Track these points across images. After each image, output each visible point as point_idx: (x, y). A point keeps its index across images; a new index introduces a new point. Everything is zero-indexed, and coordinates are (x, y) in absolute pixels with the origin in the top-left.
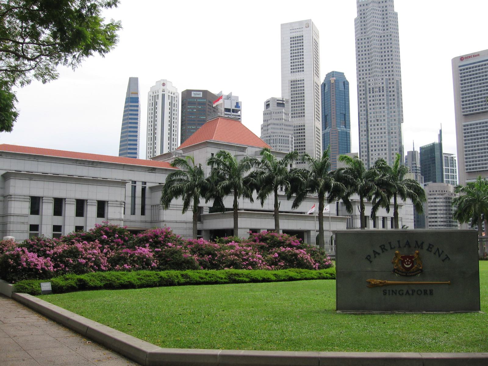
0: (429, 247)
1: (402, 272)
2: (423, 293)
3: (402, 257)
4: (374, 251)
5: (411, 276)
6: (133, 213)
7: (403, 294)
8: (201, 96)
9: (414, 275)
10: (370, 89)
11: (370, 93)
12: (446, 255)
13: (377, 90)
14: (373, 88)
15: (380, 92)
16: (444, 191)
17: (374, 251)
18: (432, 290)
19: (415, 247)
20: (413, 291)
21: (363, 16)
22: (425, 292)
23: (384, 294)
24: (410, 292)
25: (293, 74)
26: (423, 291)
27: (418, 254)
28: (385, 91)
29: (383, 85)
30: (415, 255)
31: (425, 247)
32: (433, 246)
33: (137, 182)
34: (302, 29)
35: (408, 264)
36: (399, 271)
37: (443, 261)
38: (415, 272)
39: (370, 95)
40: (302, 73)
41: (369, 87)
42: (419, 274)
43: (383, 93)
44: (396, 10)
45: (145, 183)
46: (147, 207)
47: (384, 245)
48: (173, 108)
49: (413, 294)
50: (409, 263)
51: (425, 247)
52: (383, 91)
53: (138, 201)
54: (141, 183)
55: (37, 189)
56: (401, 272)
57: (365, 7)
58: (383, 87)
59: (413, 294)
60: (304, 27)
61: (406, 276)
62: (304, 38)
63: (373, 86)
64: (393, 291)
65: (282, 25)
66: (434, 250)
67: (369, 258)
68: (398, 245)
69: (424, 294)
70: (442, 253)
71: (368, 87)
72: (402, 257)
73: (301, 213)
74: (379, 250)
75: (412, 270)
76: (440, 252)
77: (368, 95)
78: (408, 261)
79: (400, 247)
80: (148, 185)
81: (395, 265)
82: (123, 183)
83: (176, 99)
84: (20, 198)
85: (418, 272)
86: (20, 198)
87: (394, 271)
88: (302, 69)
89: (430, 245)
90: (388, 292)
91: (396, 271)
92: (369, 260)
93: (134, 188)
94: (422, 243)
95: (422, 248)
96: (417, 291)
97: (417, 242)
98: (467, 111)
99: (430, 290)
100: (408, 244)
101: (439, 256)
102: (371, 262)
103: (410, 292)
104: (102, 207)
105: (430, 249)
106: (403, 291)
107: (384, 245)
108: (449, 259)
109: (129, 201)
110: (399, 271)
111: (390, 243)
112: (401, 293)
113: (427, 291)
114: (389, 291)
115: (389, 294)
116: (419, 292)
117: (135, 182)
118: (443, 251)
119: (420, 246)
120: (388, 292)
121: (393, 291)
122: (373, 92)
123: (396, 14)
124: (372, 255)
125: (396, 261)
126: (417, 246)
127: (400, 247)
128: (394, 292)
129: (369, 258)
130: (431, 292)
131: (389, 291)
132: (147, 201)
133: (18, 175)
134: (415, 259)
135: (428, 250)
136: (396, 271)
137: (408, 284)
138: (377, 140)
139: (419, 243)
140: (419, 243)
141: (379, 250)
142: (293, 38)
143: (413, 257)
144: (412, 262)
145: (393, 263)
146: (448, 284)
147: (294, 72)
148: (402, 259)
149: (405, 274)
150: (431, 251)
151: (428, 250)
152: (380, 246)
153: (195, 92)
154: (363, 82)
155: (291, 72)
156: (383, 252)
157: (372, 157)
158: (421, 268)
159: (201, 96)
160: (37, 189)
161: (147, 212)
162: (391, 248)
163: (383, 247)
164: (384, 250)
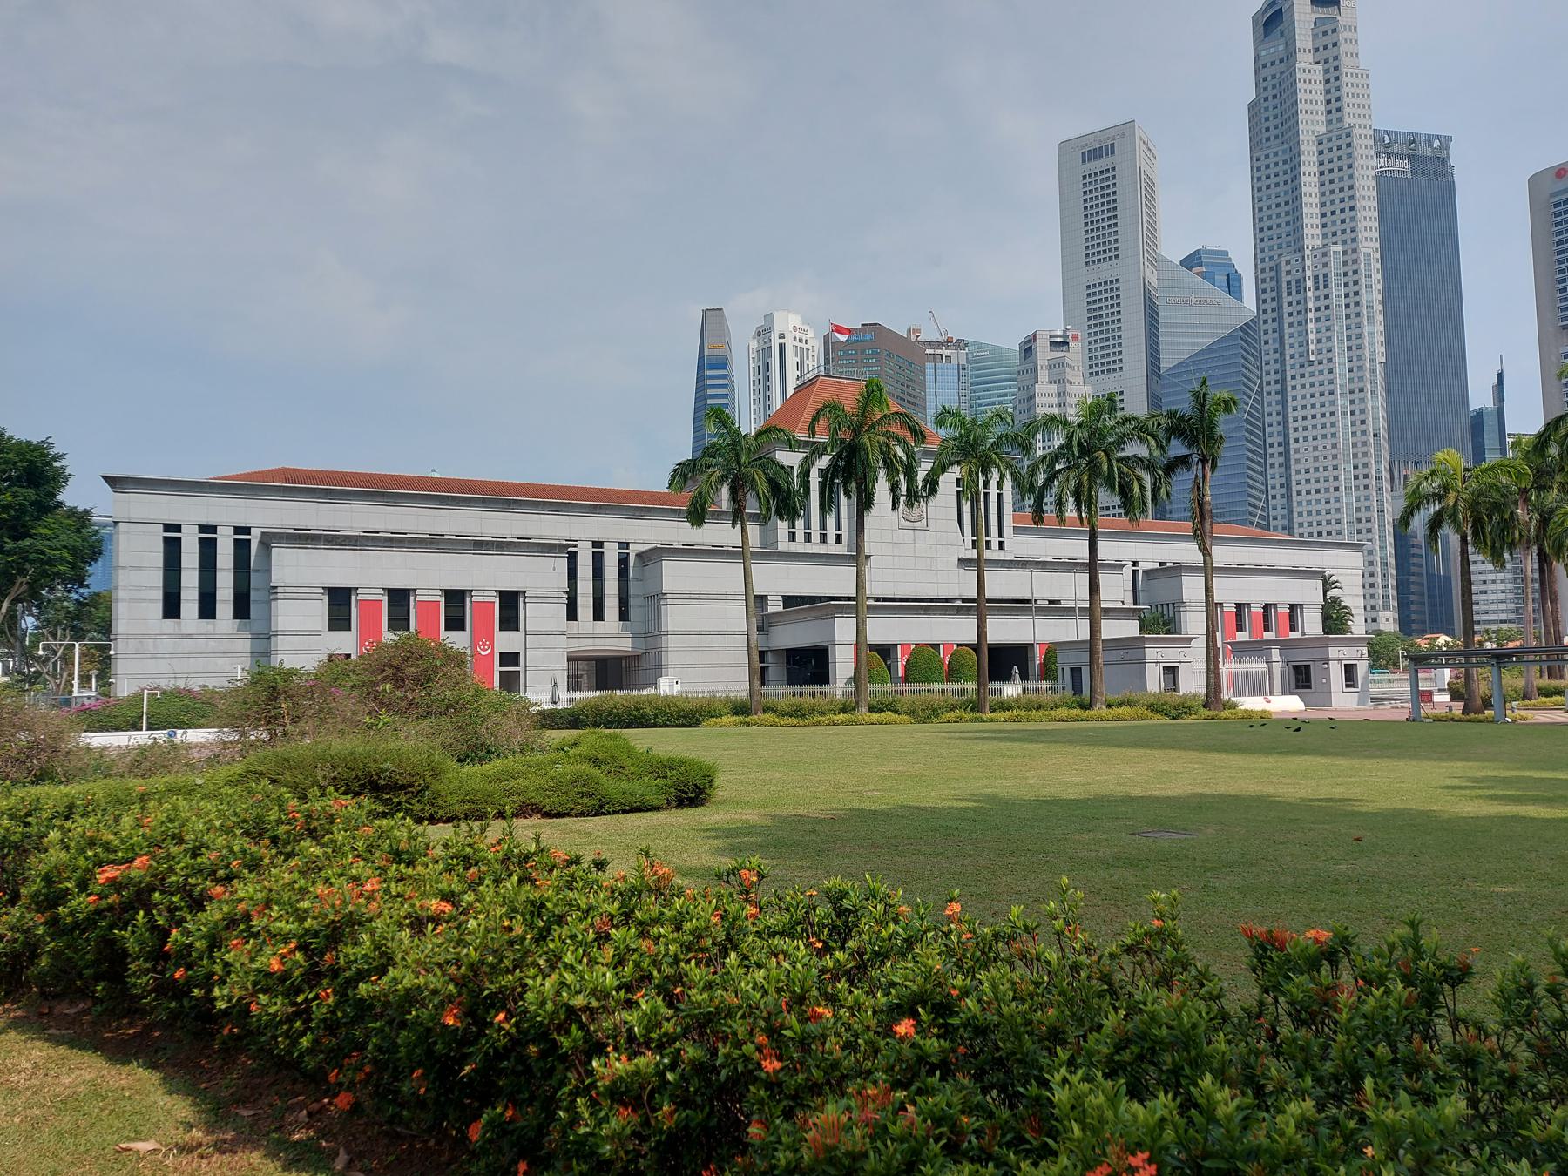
6: (598, 615)
10: (1289, 283)
11: (1289, 294)
13: (1309, 284)
14: (1298, 281)
15: (1317, 288)
29: (1325, 270)
39: (1290, 299)
41: (1289, 278)
43: (1326, 291)
46: (632, 602)
52: (1326, 286)
55: (341, 568)
58: (1326, 275)
63: (1299, 276)
71: (1285, 279)
73: (947, 600)
77: (1286, 299)
84: (301, 592)
86: (301, 592)
93: (598, 559)
109: (585, 588)
117: (598, 544)
122: (1298, 292)
132: (633, 589)
133: (304, 539)
154: (1271, 269)
160: (341, 568)
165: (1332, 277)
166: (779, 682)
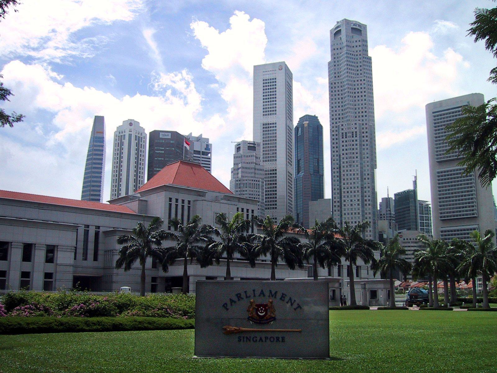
0: (282, 296)
4: (230, 299)
5: (265, 323)
7: (256, 340)
8: (170, 137)
10: (343, 133)
12: (298, 304)
14: (346, 133)
16: (407, 239)
17: (230, 299)
18: (284, 337)
19: (269, 296)
21: (336, 60)
22: (278, 339)
24: (264, 340)
25: (265, 117)
26: (275, 339)
27: (271, 303)
28: (358, 136)
29: (356, 130)
31: (279, 296)
32: (286, 295)
33: (90, 227)
34: (275, 72)
35: (261, 313)
37: (295, 309)
39: (343, 140)
40: (274, 116)
41: (342, 131)
43: (356, 138)
44: (369, 55)
45: (98, 227)
46: (100, 252)
47: (240, 294)
48: (140, 149)
49: (265, 341)
51: (279, 296)
52: (356, 136)
53: (91, 246)
54: (94, 227)
57: (339, 51)
58: (356, 132)
59: (265, 341)
60: (277, 69)
62: (277, 80)
65: (255, 67)
66: (287, 299)
67: (225, 306)
69: (277, 341)
71: (341, 131)
72: (257, 305)
74: (235, 299)
75: (265, 318)
76: (293, 302)
78: (262, 310)
79: (254, 296)
80: (102, 230)
82: (75, 228)
83: (143, 140)
87: (250, 319)
88: (274, 112)
89: (283, 294)
90: (242, 338)
93: (86, 233)
94: (276, 292)
95: (275, 297)
97: (271, 292)
98: (441, 158)
99: (282, 338)
100: (262, 293)
102: (227, 309)
103: (264, 340)
104: (51, 250)
105: (283, 299)
106: (256, 337)
107: (240, 294)
108: (301, 308)
109: (81, 245)
111: (246, 292)
115: (244, 341)
116: (272, 339)
117: (88, 226)
119: (273, 295)
120: (242, 338)
121: (247, 338)
122: (346, 137)
123: (370, 59)
124: (229, 303)
125: (251, 309)
127: (254, 296)
130: (283, 339)
132: (101, 246)
135: (281, 299)
137: (261, 331)
138: (349, 186)
139: (273, 292)
140: (273, 292)
141: (235, 299)
142: (266, 80)
143: (266, 305)
144: (266, 311)
145: (248, 311)
147: (266, 114)
149: (259, 322)
150: (283, 300)
152: (237, 295)
153: (163, 133)
155: (264, 115)
156: (239, 300)
157: (345, 203)
158: (274, 316)
159: (170, 137)
161: (100, 257)
162: (247, 297)
163: (239, 295)
165: (358, 133)
166: (162, 291)
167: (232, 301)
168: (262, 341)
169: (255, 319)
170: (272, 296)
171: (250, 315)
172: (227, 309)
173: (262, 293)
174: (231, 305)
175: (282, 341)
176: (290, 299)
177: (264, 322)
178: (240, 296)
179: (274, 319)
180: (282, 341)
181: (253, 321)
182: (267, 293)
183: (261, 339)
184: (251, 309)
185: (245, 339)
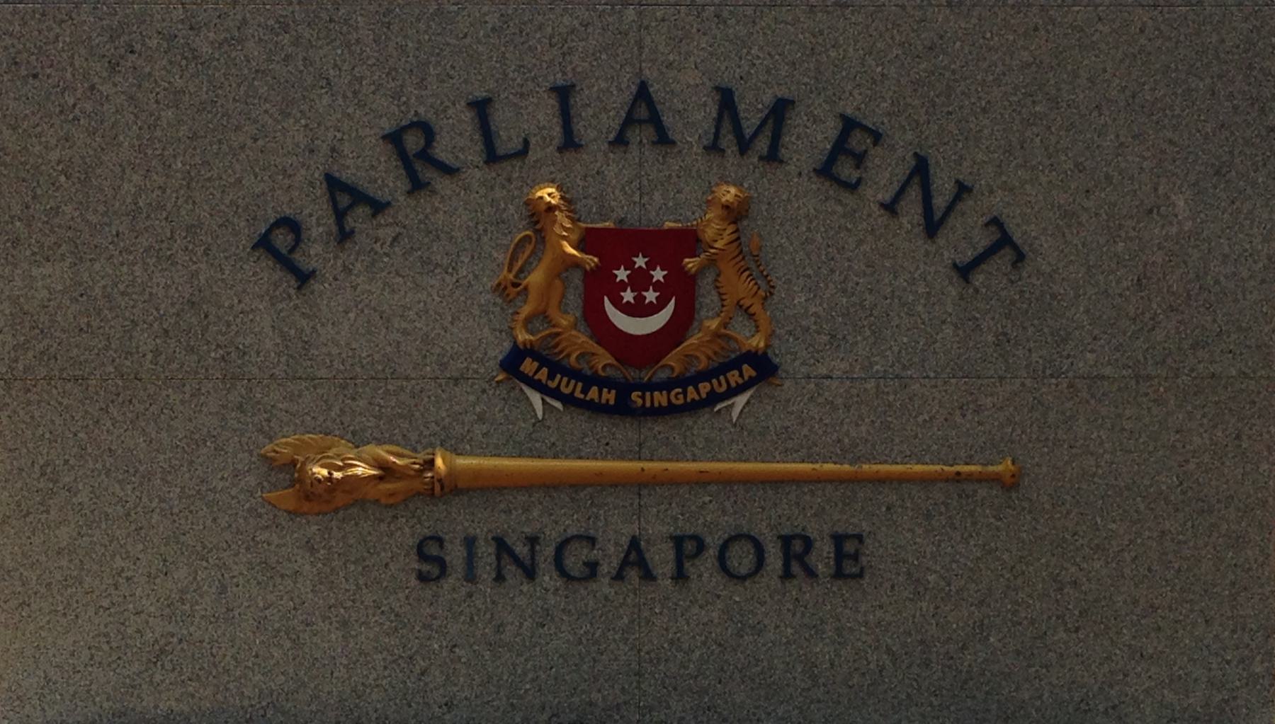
0: (840, 147)
1: (590, 380)
2: (774, 560)
3: (588, 241)
4: (334, 184)
5: (671, 410)
9: (692, 407)
12: (996, 222)
17: (334, 184)
20: (686, 548)
22: (796, 550)
23: (423, 578)
24: (661, 557)
27: (735, 214)
30: (715, 231)
35: (639, 309)
36: (556, 368)
37: (964, 271)
38: (706, 375)
42: (741, 400)
49: (680, 576)
50: (651, 296)
51: (810, 136)
56: (574, 374)
59: (680, 576)
61: (622, 409)
64: (501, 545)
66: (885, 172)
68: (557, 131)
69: (787, 575)
70: (950, 209)
78: (640, 280)
79: (570, 143)
81: (526, 310)
85: (734, 377)
89: (849, 125)
91: (528, 366)
92: (286, 262)
94: (780, 110)
95: (773, 157)
96: (722, 558)
97: (727, 100)
99: (838, 540)
100: (644, 115)
101: (932, 227)
102: (303, 278)
103: (661, 557)
105: (846, 170)
106: (592, 541)
107: (426, 129)
108: (1020, 257)
110: (556, 368)
111: (481, 108)
112: (575, 559)
113: (808, 543)
114: (470, 542)
115: (471, 577)
116: (741, 559)
118: (962, 190)
120: (455, 554)
121: (501, 545)
125: (536, 278)
126: (728, 141)
127: (570, 143)
128: (515, 559)
129: (282, 240)
131: (470, 542)
134: (712, 261)
135: (825, 171)
136: (528, 366)
137: (641, 484)
141: (385, 178)
143: (688, 240)
146: (995, 479)
148: (592, 260)
149: (609, 396)
150: (852, 187)
151: (825, 171)
152: (394, 138)
156: (417, 186)
158: (757, 342)
162: (492, 157)
163: (413, 142)
164: (428, 174)
167: (345, 197)
168: (648, 575)
169: (574, 374)
170: (744, 147)
171: (523, 336)
172: (303, 278)
173: (644, 115)
174: (344, 236)
175: (839, 574)
176: (921, 169)
177: (660, 398)
178: (425, 155)
179: (763, 368)
180: (839, 574)
181: (556, 394)
182: (692, 116)
183: (635, 558)
184: (536, 278)
185: (486, 571)
